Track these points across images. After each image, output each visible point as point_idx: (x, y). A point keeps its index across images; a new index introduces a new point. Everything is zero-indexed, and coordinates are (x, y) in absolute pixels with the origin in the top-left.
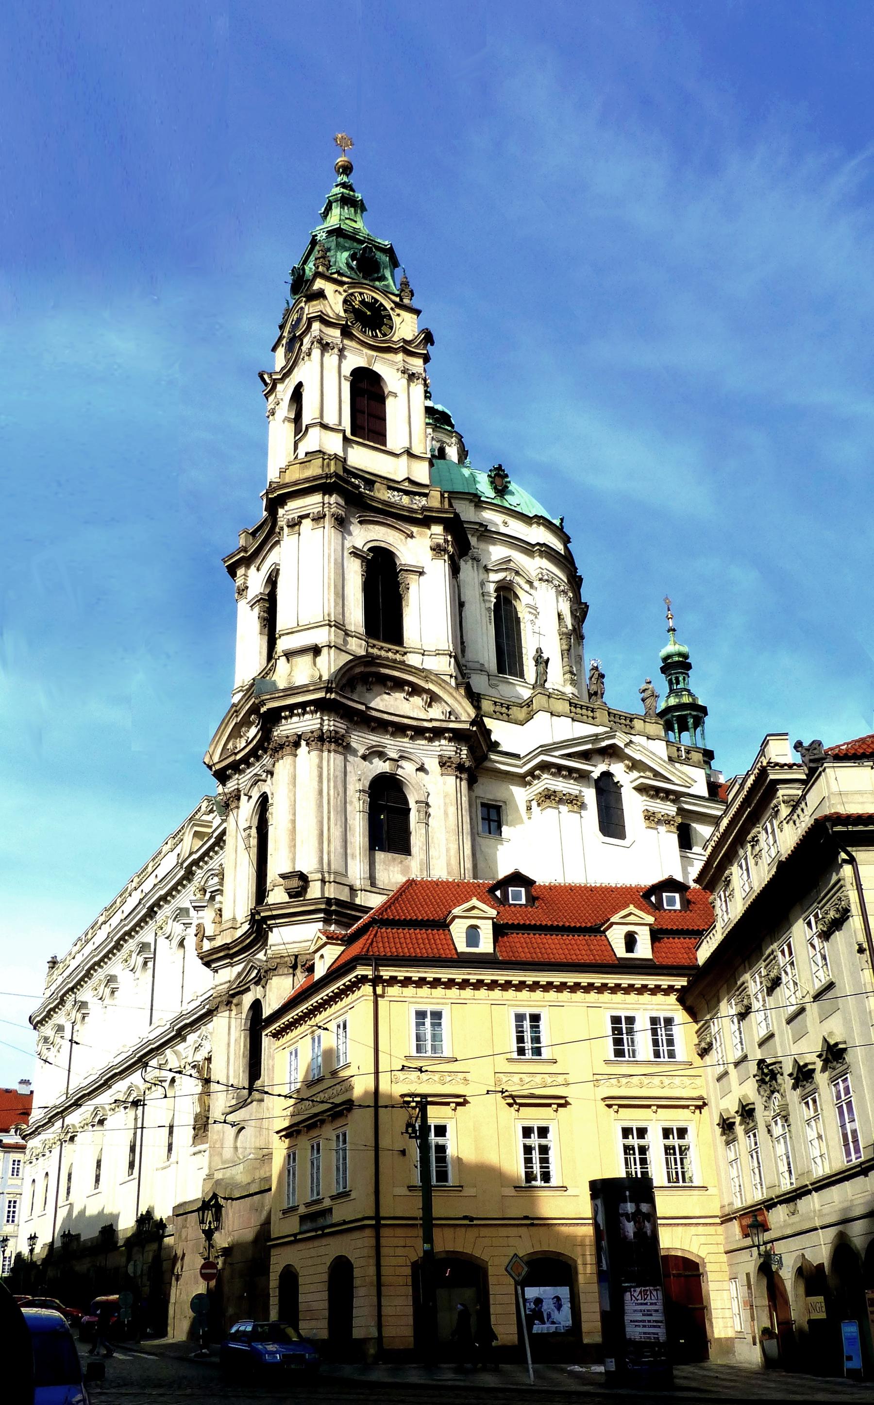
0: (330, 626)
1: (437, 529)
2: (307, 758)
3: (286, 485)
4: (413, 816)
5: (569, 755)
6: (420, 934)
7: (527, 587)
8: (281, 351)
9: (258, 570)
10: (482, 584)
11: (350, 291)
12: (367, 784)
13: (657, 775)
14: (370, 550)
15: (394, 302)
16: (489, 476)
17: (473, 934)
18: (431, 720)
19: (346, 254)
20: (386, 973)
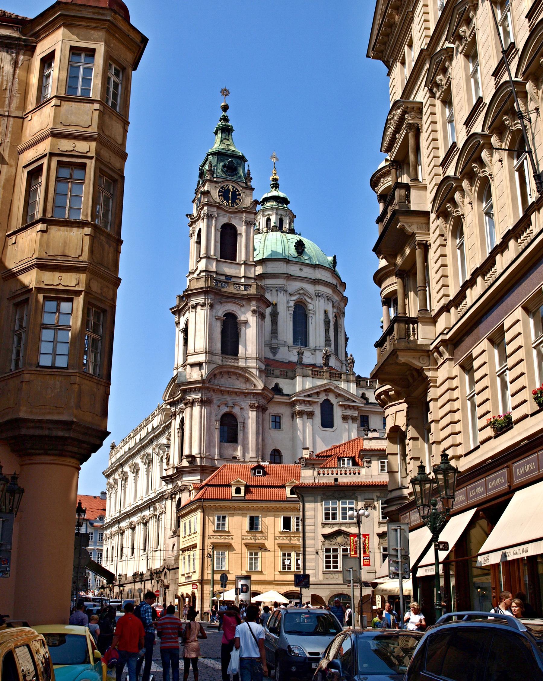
0: (206, 353)
1: (254, 303)
2: (197, 409)
3: (191, 290)
4: (239, 428)
5: (309, 396)
6: (221, 489)
7: (309, 301)
8: (195, 205)
9: (183, 316)
10: (288, 302)
11: (222, 185)
12: (219, 417)
13: (349, 399)
14: (224, 316)
15: (243, 187)
16: (295, 246)
17: (238, 491)
18: (246, 389)
19: (222, 164)
20: (207, 504)
